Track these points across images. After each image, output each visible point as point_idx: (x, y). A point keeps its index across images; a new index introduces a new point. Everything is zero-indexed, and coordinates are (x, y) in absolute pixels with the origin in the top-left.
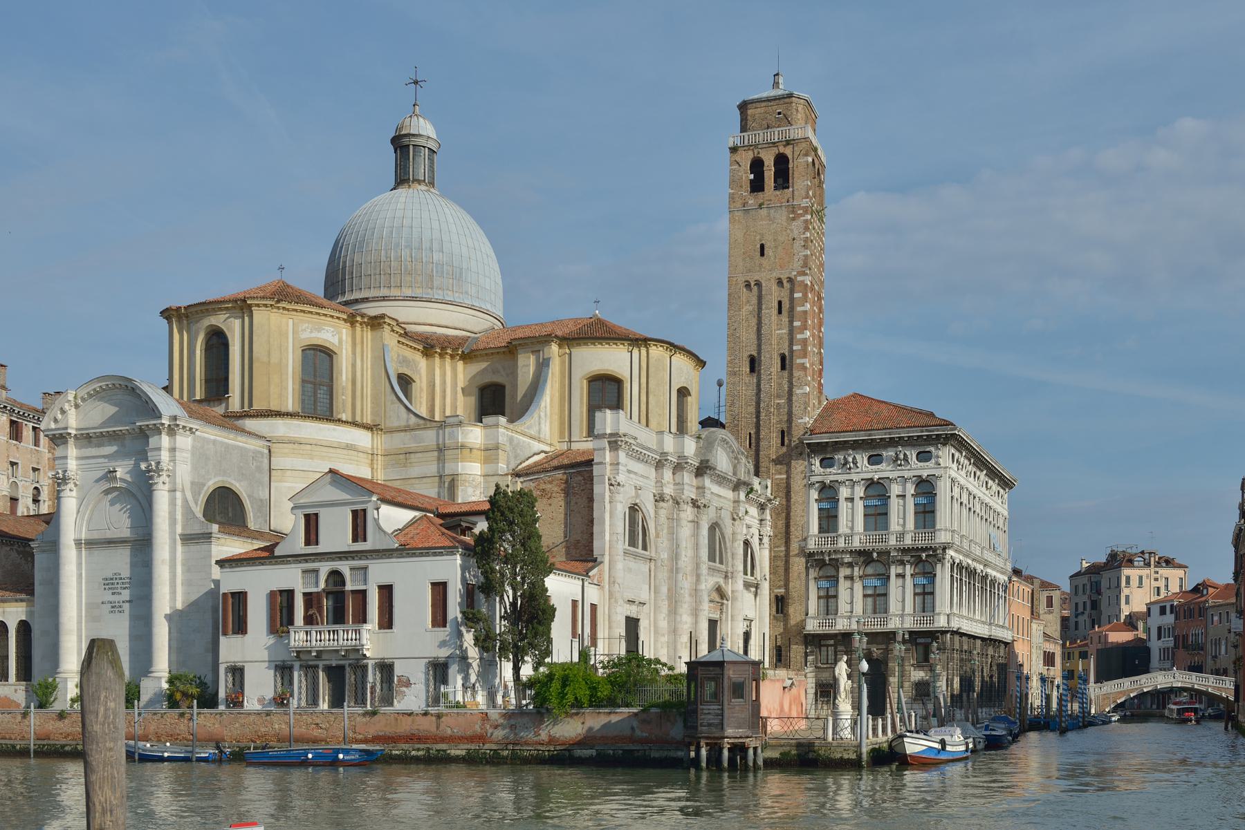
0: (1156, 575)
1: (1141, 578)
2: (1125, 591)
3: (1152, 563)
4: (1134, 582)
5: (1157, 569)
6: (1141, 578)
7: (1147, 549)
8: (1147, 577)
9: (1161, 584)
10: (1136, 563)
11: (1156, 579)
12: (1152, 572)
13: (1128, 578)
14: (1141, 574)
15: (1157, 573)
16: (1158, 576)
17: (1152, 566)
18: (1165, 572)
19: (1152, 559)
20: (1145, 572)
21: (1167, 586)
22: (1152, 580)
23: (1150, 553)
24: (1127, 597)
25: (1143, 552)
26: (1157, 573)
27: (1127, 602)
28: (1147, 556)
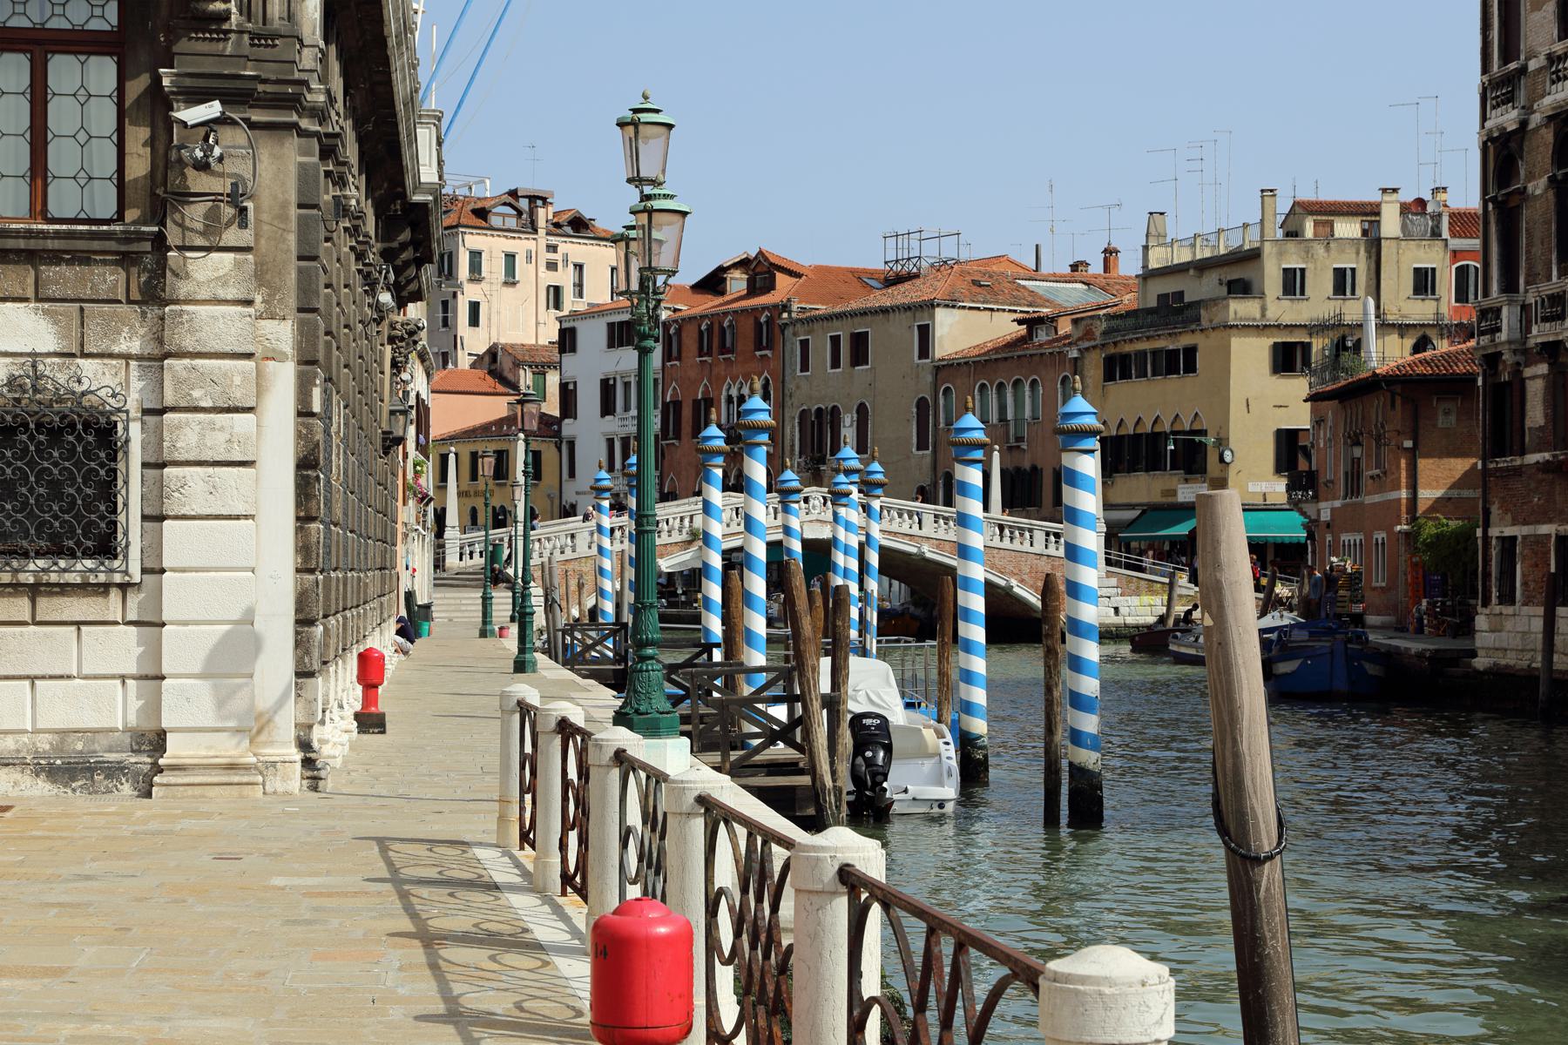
0: (551, 256)
1: (510, 258)
2: (470, 293)
3: (541, 223)
4: (493, 267)
5: (553, 240)
6: (510, 258)
7: (527, 185)
8: (529, 258)
9: (566, 278)
10: (495, 221)
11: (552, 266)
12: (543, 247)
13: (476, 256)
14: (510, 250)
15: (552, 248)
16: (558, 257)
17: (542, 232)
18: (575, 249)
19: (541, 212)
20: (520, 246)
21: (579, 287)
22: (542, 268)
23: (532, 199)
24: (475, 308)
25: (513, 194)
26: (552, 248)
27: (474, 321)
28: (524, 204)
